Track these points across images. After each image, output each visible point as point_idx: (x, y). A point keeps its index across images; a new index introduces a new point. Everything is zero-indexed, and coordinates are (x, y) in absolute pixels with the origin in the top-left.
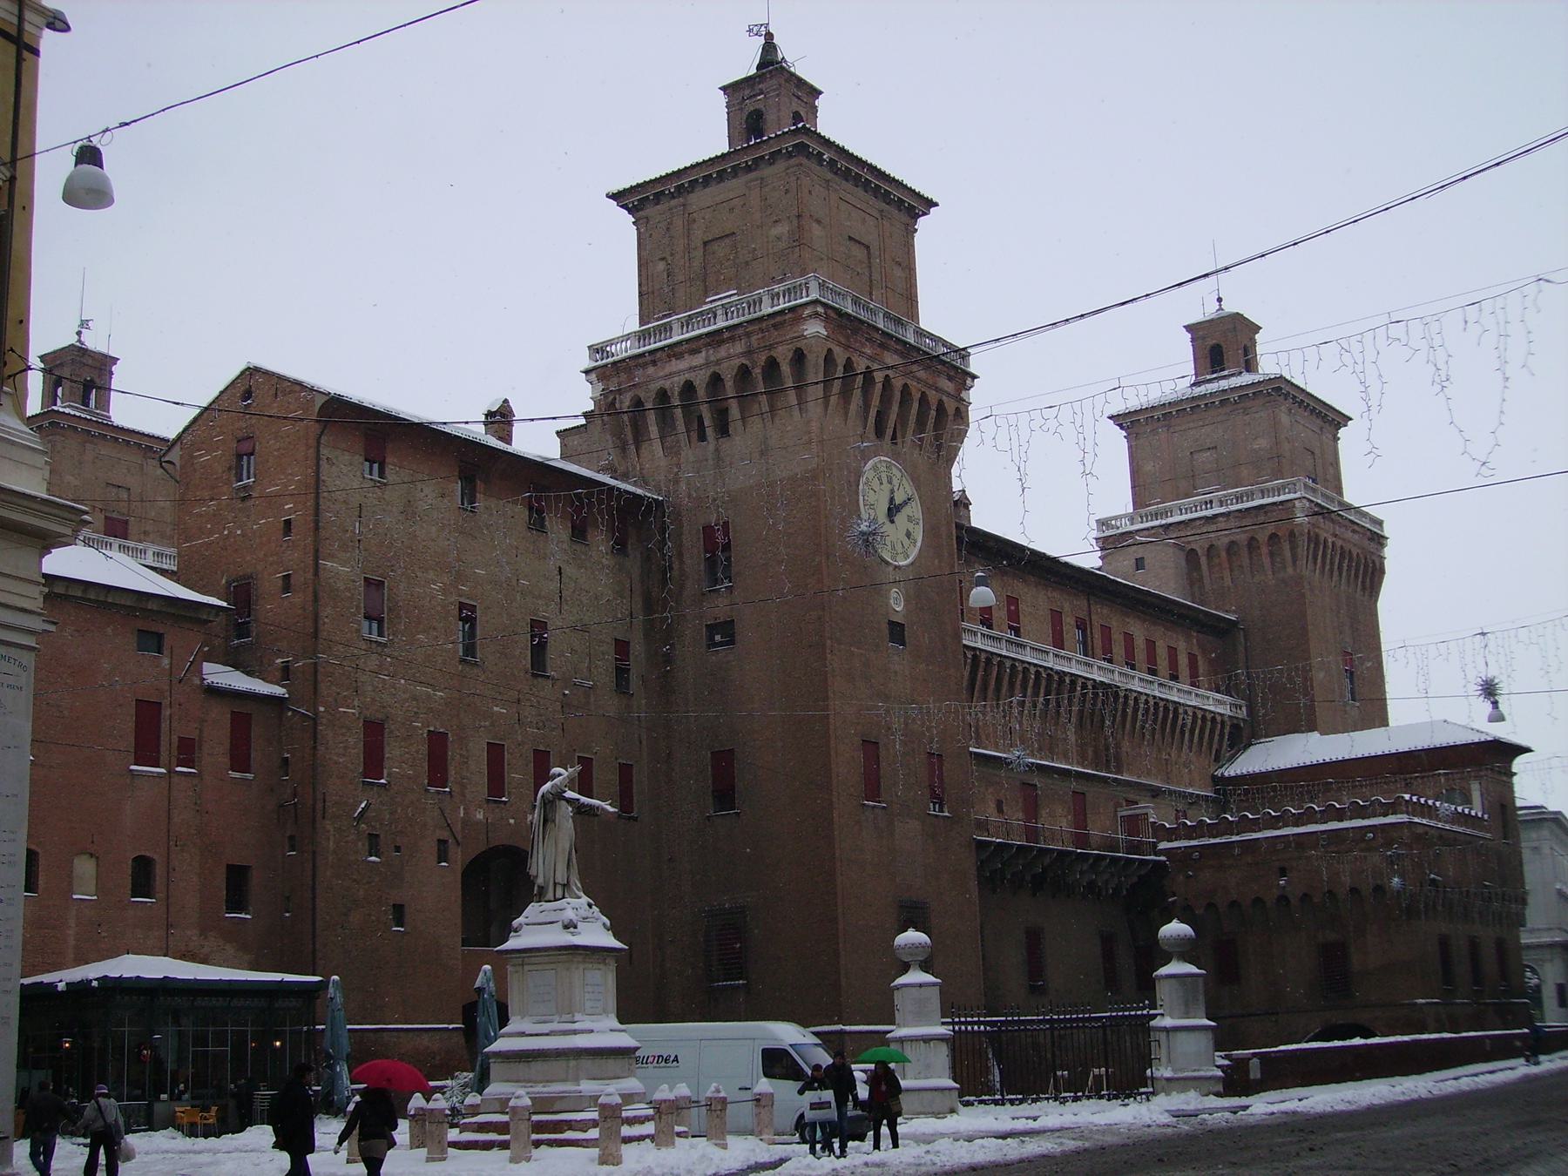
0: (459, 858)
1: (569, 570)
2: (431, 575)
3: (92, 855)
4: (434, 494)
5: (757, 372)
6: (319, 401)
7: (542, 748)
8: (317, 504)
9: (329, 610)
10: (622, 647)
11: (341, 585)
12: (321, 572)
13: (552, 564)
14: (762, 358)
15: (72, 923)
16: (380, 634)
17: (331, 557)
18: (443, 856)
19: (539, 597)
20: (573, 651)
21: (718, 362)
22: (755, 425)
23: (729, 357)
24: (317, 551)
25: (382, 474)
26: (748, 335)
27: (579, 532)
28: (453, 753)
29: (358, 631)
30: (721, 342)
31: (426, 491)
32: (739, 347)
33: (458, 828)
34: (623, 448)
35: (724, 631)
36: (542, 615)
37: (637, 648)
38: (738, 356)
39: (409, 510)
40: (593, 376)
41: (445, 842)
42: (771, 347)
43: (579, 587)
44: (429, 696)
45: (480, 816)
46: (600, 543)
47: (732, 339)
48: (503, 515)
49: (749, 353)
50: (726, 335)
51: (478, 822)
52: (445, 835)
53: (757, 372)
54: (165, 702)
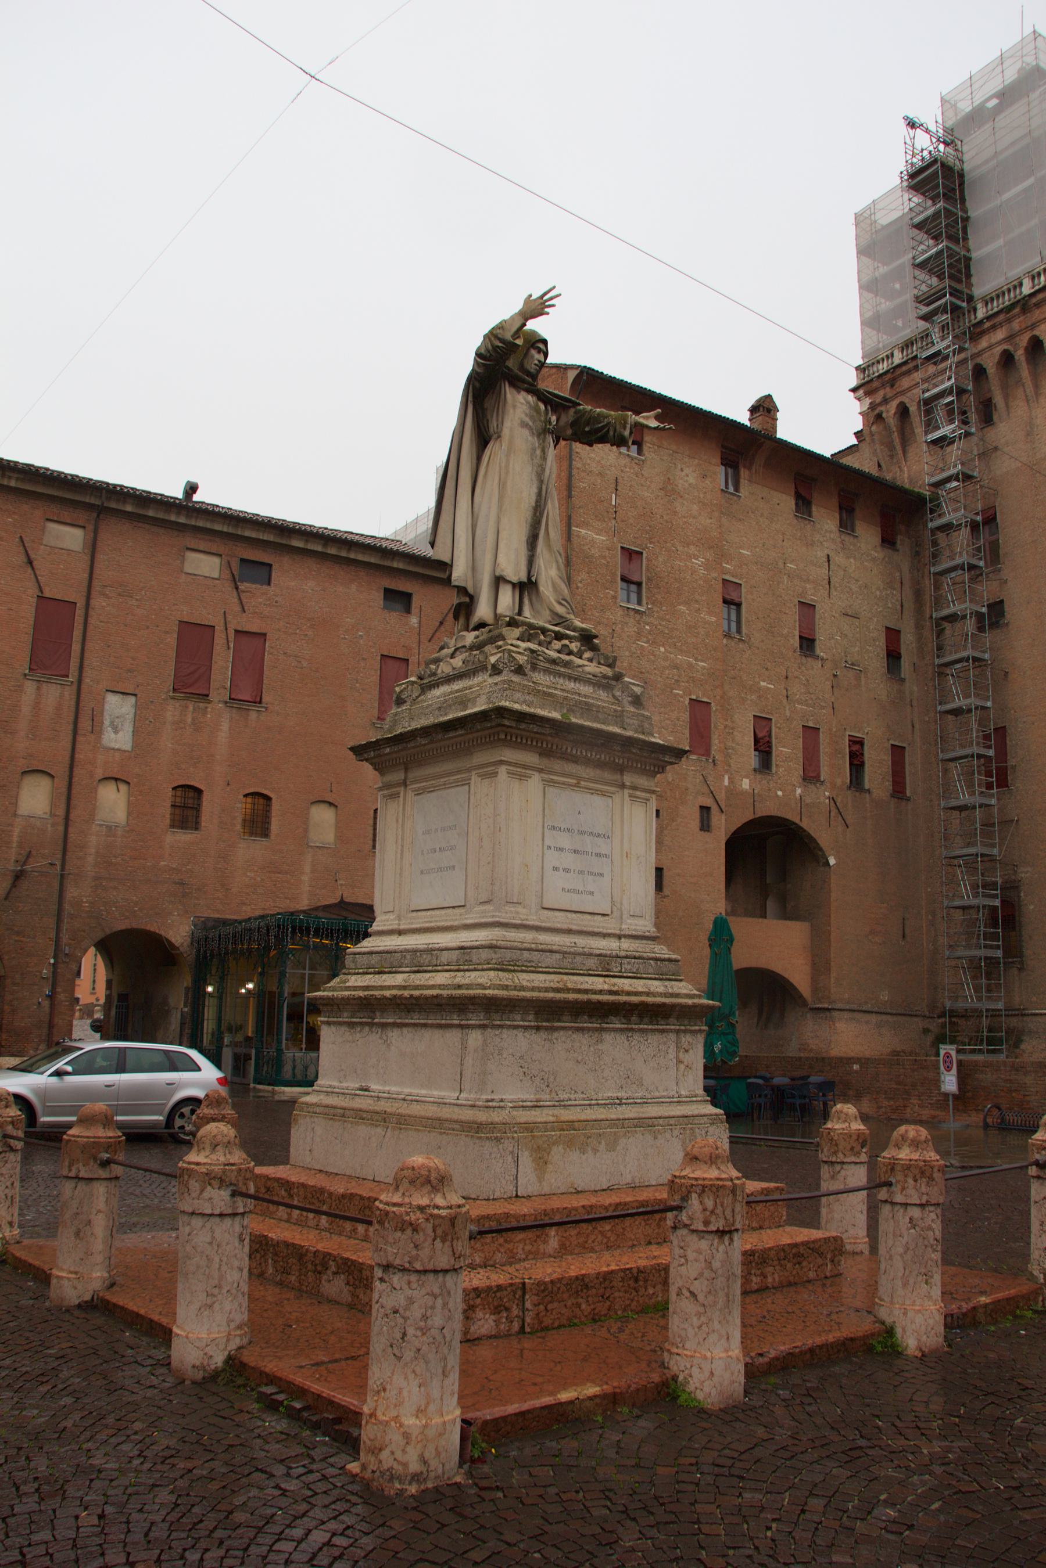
0: (723, 827)
1: (838, 559)
2: (692, 549)
3: (331, 804)
4: (696, 474)
5: (1020, 355)
6: (572, 375)
7: (811, 724)
8: (570, 477)
9: (583, 575)
10: (893, 635)
11: (595, 552)
12: (575, 540)
13: (821, 554)
14: (1024, 340)
15: (307, 869)
16: (639, 603)
17: (585, 525)
18: (705, 826)
19: (808, 580)
20: (844, 635)
21: (979, 354)
22: (1019, 408)
23: (990, 347)
24: (570, 517)
25: (640, 452)
26: (1009, 321)
27: (846, 526)
28: (717, 721)
29: (615, 597)
30: (983, 333)
31: (686, 471)
32: (1000, 334)
33: (721, 796)
34: (891, 447)
35: (994, 615)
36: (809, 598)
37: (908, 641)
38: (1000, 343)
39: (669, 489)
40: (861, 392)
41: (708, 809)
42: (1033, 326)
43: (844, 573)
44: (690, 665)
45: (746, 784)
46: (868, 536)
47: (994, 327)
48: (769, 503)
49: (1010, 338)
50: (987, 325)
51: (744, 793)
52: (708, 802)
53: (1020, 355)
54: (414, 659)
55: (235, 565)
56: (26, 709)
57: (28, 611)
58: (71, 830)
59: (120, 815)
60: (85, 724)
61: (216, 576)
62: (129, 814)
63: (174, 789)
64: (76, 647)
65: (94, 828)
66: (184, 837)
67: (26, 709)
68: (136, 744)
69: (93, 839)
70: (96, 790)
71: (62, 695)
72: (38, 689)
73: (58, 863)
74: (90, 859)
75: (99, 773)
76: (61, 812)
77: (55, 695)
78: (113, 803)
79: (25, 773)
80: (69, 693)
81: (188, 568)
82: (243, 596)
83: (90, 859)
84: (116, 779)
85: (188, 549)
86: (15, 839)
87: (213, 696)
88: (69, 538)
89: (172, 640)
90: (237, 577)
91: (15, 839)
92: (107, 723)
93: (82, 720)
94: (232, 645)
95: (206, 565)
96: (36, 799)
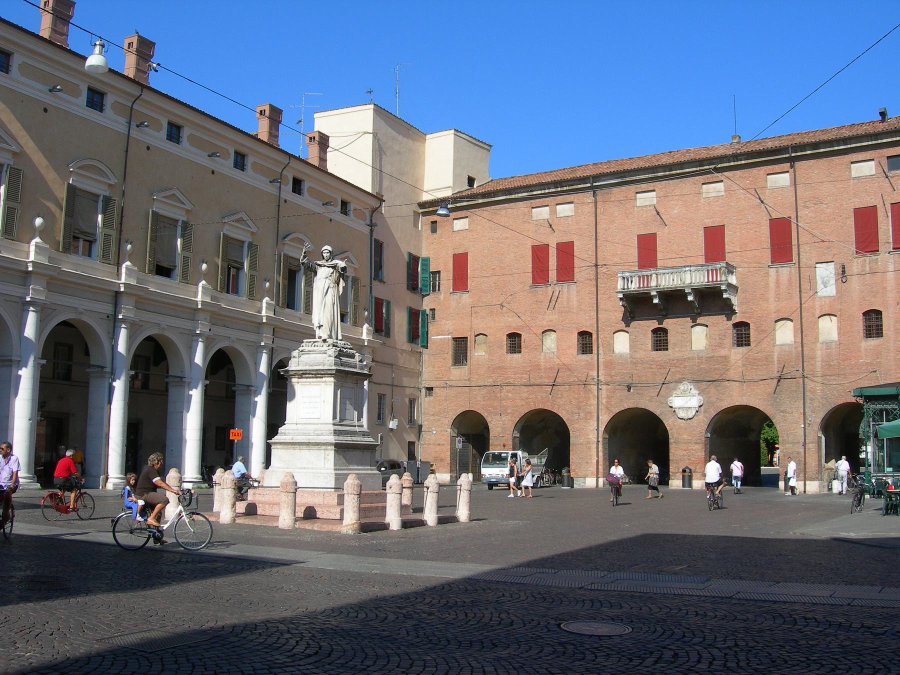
55: (885, 162)
56: (772, 285)
57: (766, 231)
58: (805, 349)
59: (834, 336)
60: (805, 286)
61: (874, 173)
62: (839, 334)
63: (865, 314)
64: (794, 242)
65: (819, 346)
66: (873, 342)
67: (772, 285)
68: (837, 292)
69: (819, 353)
70: (817, 323)
71: (790, 272)
72: (777, 272)
73: (801, 369)
74: (819, 364)
75: (818, 313)
76: (799, 340)
77: (786, 272)
78: (828, 329)
79: (776, 322)
80: (794, 270)
81: (854, 174)
82: (892, 180)
83: (819, 364)
84: (829, 315)
85: (852, 163)
86: (776, 359)
87: (881, 248)
88: (781, 180)
89: (851, 222)
90: (886, 170)
91: (776, 359)
92: (819, 282)
93: (804, 285)
94: (890, 214)
95: (865, 168)
96: (785, 334)
